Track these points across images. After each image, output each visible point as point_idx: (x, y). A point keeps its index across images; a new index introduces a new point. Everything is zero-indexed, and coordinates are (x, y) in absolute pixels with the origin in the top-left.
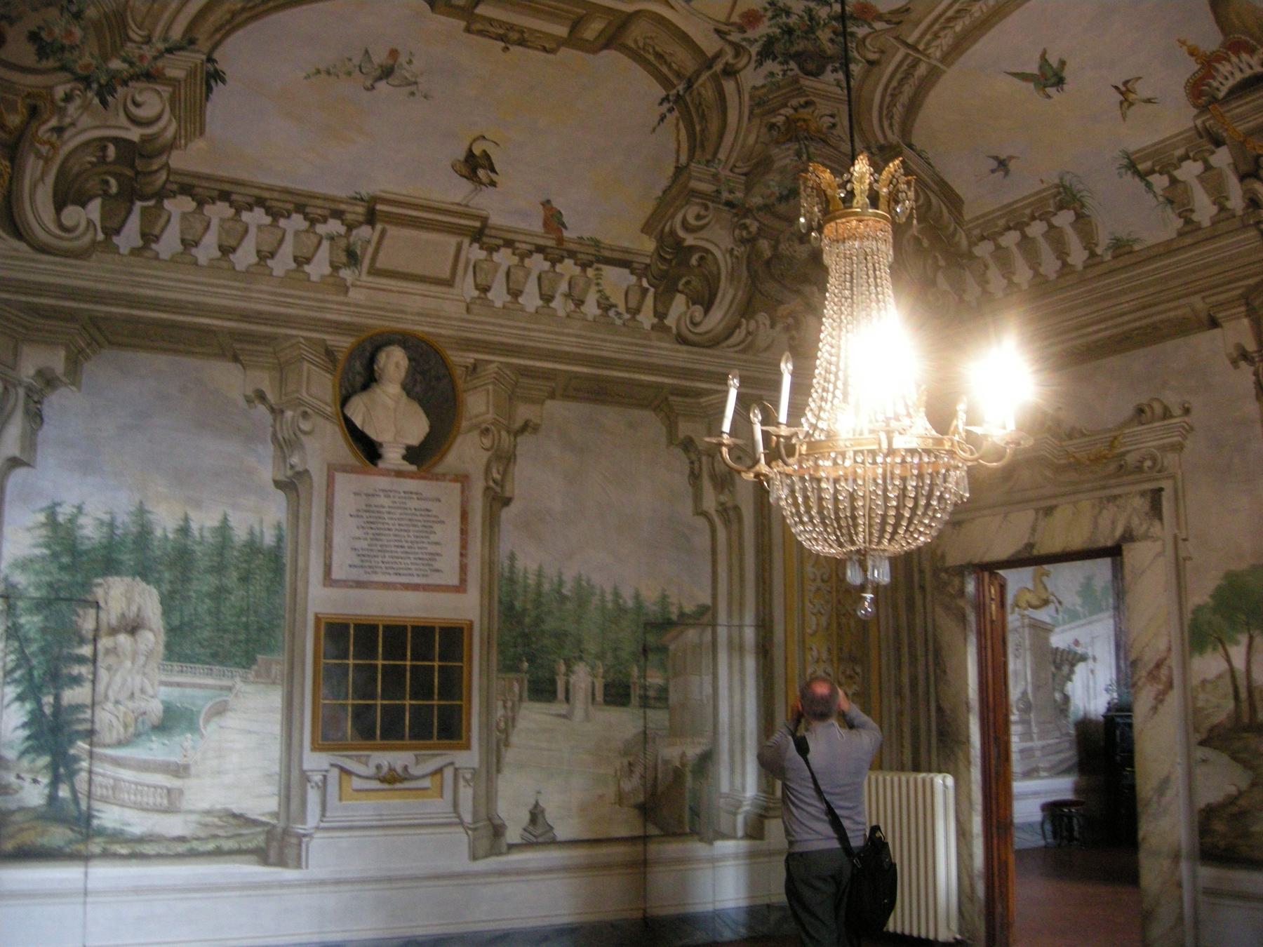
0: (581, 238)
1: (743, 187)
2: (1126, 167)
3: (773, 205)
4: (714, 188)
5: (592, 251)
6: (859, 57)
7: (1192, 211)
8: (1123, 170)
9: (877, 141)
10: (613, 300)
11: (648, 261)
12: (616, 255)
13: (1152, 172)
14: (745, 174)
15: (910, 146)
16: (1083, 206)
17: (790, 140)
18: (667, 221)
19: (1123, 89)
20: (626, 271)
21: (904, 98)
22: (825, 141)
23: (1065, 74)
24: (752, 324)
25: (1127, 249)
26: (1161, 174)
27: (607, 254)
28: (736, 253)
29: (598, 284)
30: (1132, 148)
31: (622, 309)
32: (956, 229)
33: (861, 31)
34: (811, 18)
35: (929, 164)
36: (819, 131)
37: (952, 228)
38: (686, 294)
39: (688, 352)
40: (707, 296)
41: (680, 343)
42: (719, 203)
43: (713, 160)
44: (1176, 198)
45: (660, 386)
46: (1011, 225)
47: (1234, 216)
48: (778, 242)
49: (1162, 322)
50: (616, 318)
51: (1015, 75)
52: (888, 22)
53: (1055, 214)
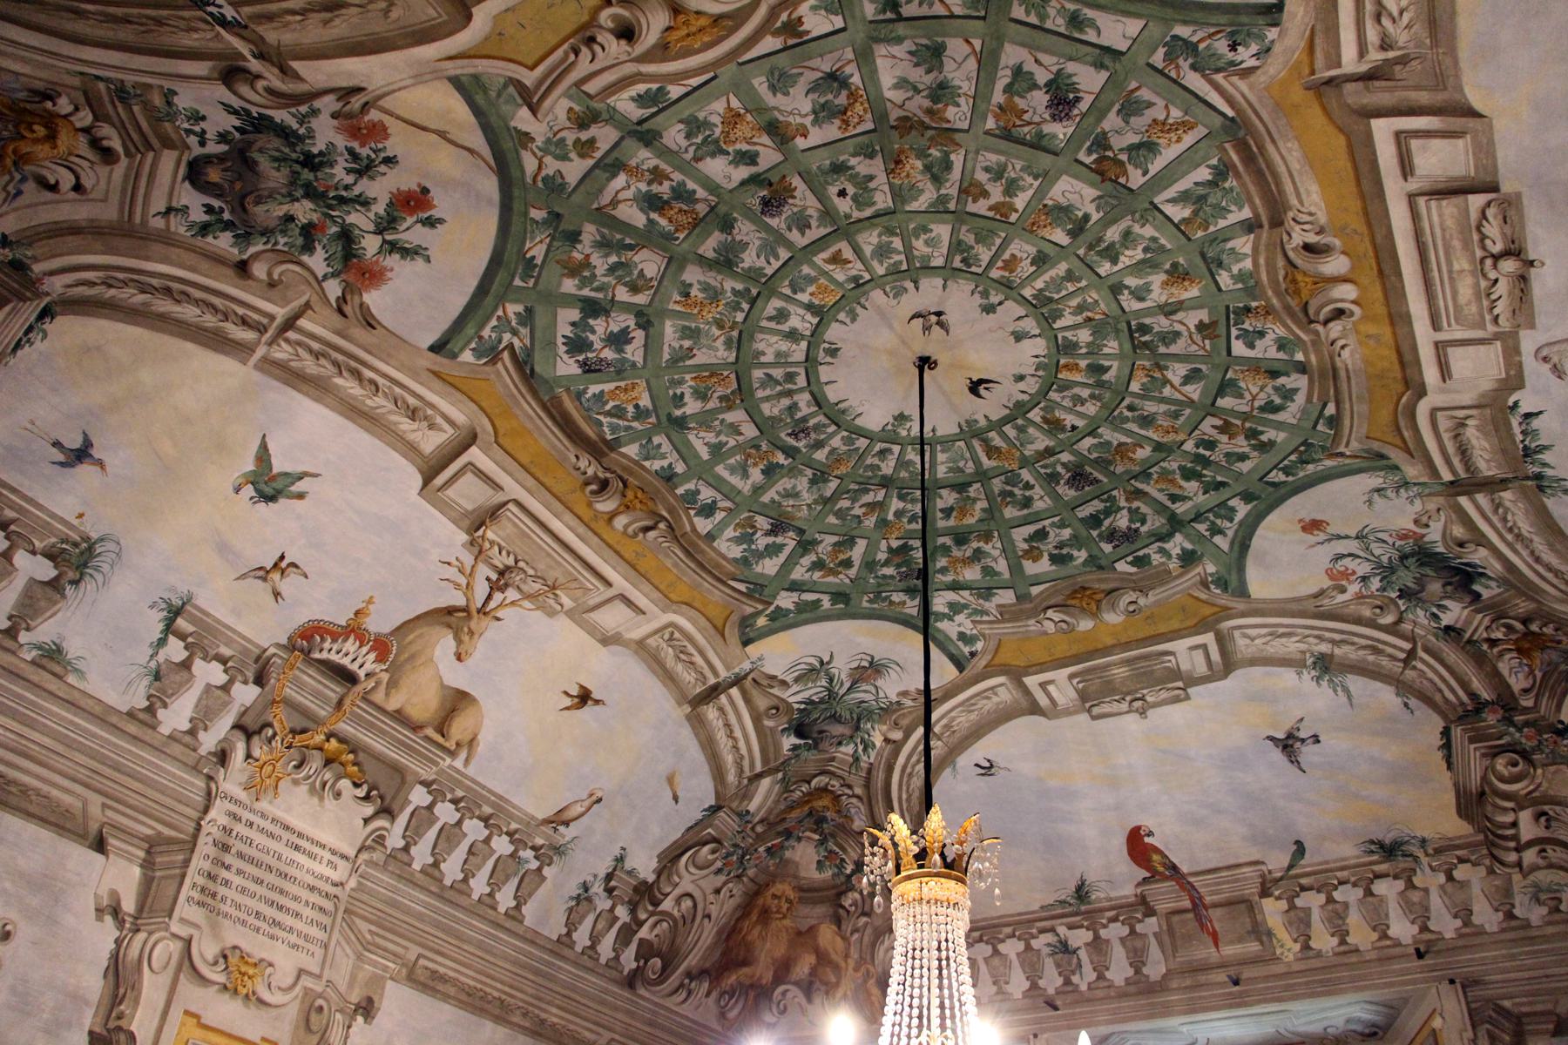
2: (170, 605)
6: (252, 250)
7: (165, 706)
8: (164, 606)
9: (36, 259)
13: (182, 636)
15: (46, 313)
16: (76, 583)
19: (283, 564)
21: (164, 306)
23: (283, 502)
25: (58, 669)
26: (186, 648)
30: (201, 601)
33: (317, 261)
34: (342, 201)
35: (18, 346)
44: (164, 681)
47: (195, 750)
49: (38, 793)
51: (264, 447)
52: (343, 299)
53: (34, 553)
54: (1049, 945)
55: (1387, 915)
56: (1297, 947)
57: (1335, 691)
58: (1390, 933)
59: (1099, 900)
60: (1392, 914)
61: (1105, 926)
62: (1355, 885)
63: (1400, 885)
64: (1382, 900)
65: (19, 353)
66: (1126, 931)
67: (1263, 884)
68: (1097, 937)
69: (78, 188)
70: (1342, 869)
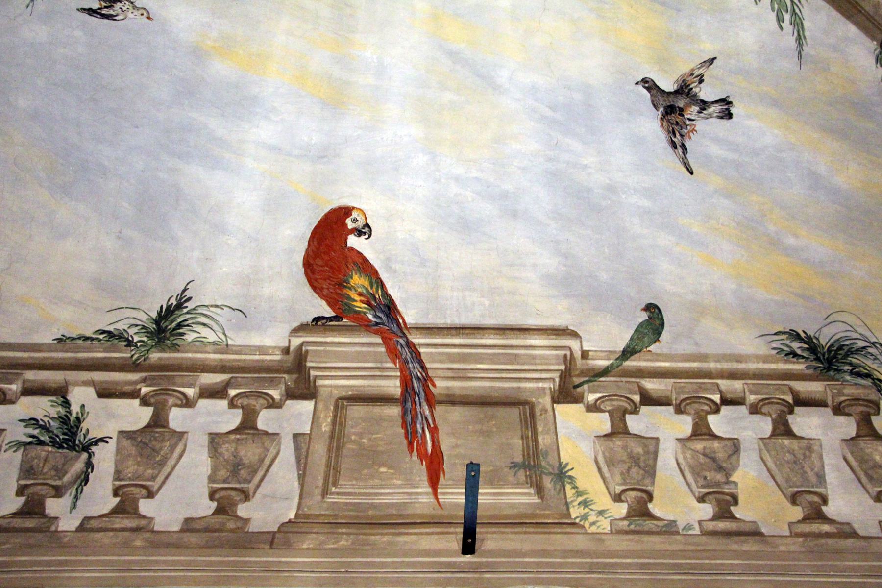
54: (33, 422)
55: (821, 478)
56: (622, 509)
57: (780, 19)
58: (829, 510)
59: (201, 345)
60: (831, 477)
61: (188, 403)
62: (755, 410)
63: (847, 426)
64: (809, 446)
66: (233, 419)
67: (565, 375)
68: (158, 422)
70: (733, 375)
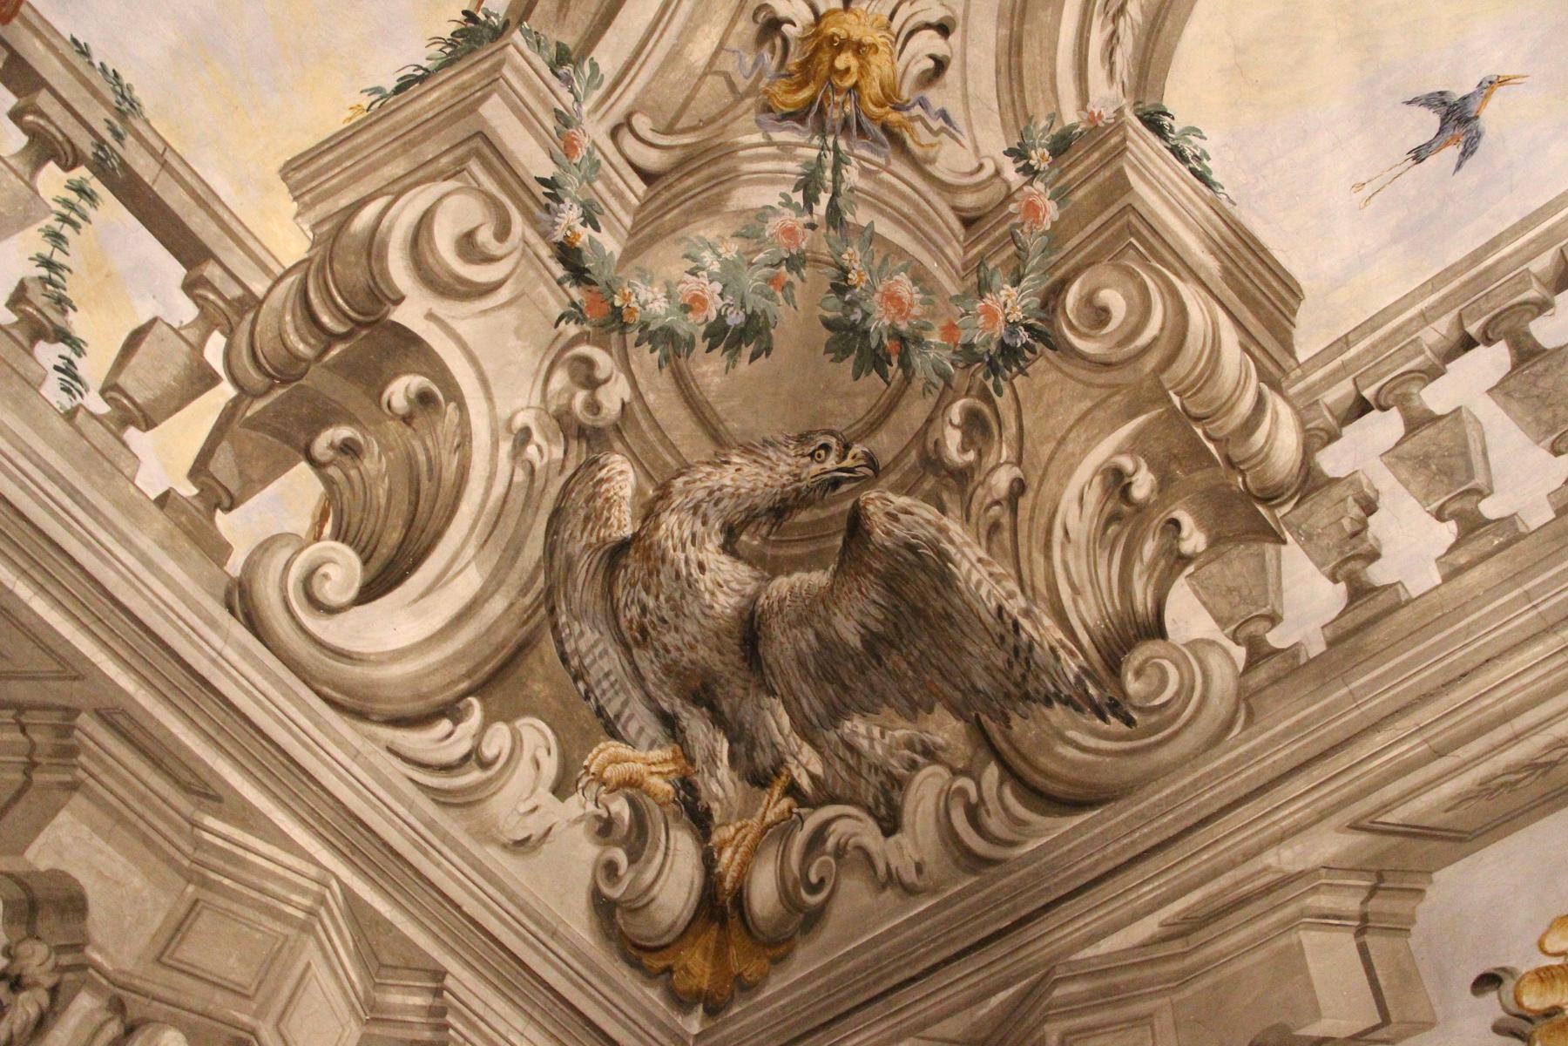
0: (84, 52)
1: (628, 221)
3: (691, 344)
4: (548, 170)
5: (98, 117)
9: (1053, 117)
10: (77, 323)
11: (259, 288)
12: (175, 198)
14: (647, 177)
15: (1154, 121)
17: (797, 116)
18: (371, 198)
20: (178, 271)
22: (895, 139)
24: (498, 741)
27: (144, 166)
28: (531, 450)
29: (56, 238)
31: (94, 367)
32: (1260, 402)
35: (1202, 177)
36: (890, 97)
37: (1246, 404)
38: (328, 482)
39: (246, 653)
40: (394, 537)
41: (232, 611)
42: (544, 235)
43: (577, 64)
45: (73, 668)
46: (1473, 329)
48: (664, 492)
50: (54, 379)
65: (1215, 177)
69: (944, 29)
